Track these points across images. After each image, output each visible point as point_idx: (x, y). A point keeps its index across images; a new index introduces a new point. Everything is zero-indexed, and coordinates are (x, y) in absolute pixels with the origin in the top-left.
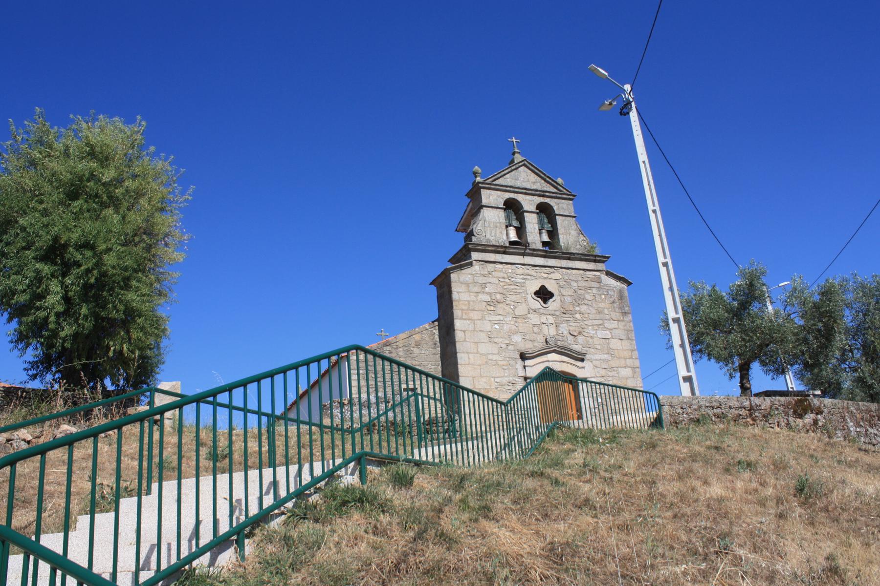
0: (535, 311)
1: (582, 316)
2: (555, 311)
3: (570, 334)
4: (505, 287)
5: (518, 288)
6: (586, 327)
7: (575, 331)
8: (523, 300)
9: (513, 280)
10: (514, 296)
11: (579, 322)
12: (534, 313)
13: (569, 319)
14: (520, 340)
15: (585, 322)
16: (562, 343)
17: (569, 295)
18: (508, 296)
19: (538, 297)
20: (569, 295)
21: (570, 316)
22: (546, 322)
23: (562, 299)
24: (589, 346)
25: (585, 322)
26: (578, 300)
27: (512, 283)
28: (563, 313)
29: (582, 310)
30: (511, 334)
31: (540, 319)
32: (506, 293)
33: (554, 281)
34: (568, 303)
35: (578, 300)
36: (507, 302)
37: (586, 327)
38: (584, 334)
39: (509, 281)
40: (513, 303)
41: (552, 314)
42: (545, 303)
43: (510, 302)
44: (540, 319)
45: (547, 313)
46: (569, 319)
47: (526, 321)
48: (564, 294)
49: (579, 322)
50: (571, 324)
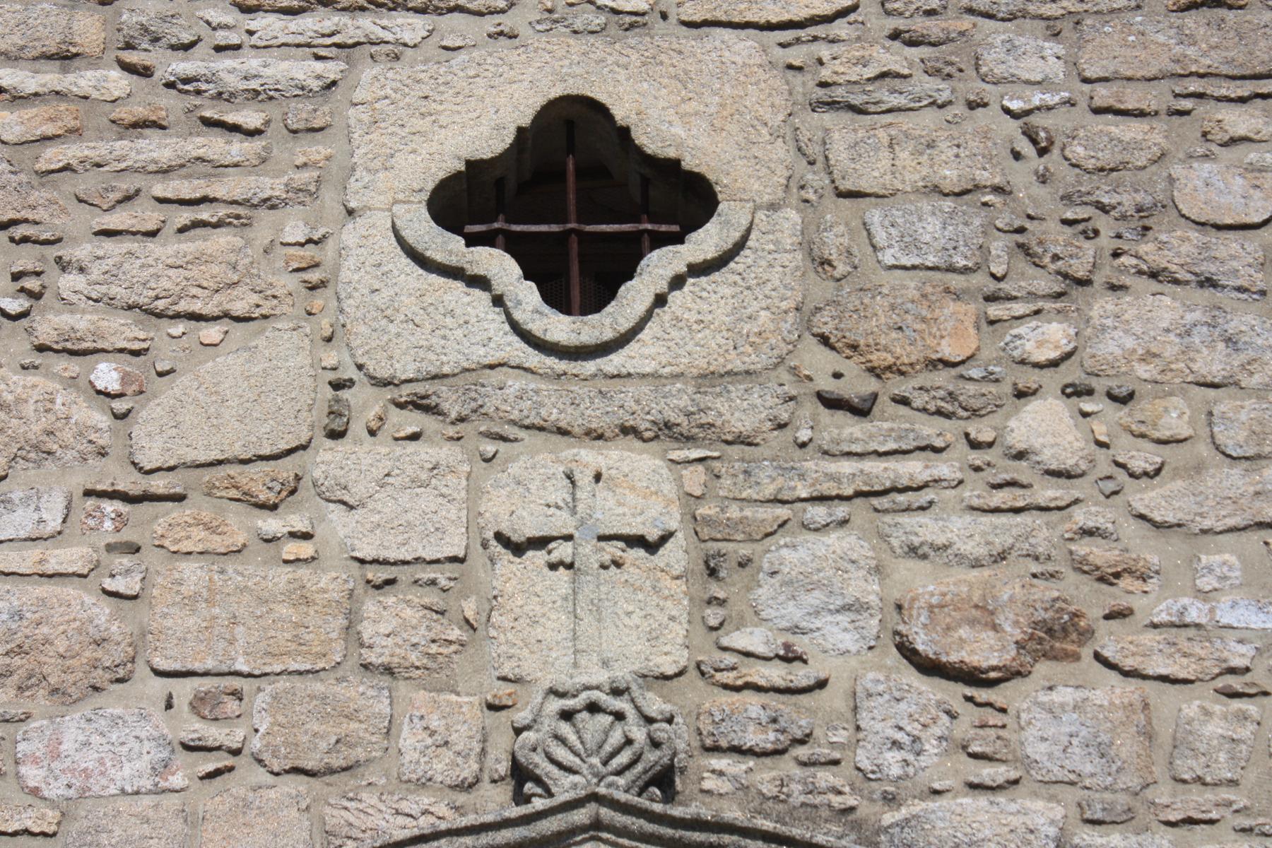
0: (421, 405)
1: (1108, 418)
2: (709, 379)
3: (908, 652)
4: (53, 156)
5: (238, 148)
6: (1150, 551)
7: (985, 615)
8: (288, 283)
9: (183, 66)
10: (166, 250)
11: (1048, 492)
12: (412, 421)
13: (913, 469)
14: (134, 772)
15: (1148, 498)
16: (765, 777)
17: (937, 190)
18: (81, 251)
19: (472, 241)
20: (937, 190)
21: (930, 429)
22: (561, 522)
23: (833, 242)
24: (1196, 801)
25: (1148, 498)
26: (1057, 238)
27: (170, 105)
28: (832, 403)
29: (1111, 346)
30: (40, 701)
31: (474, 492)
32: (52, 222)
33: (743, 46)
34: (911, 283)
35: (1057, 238)
36: (48, 325)
37: (1150, 551)
38: (1111, 641)
39: (118, 82)
40: (124, 330)
41: (666, 430)
42: (557, 298)
43: (82, 322)
44: (474, 492)
45: (596, 414)
46: (913, 469)
47: (272, 524)
48: (869, 176)
49: (1048, 492)
50: (925, 528)
